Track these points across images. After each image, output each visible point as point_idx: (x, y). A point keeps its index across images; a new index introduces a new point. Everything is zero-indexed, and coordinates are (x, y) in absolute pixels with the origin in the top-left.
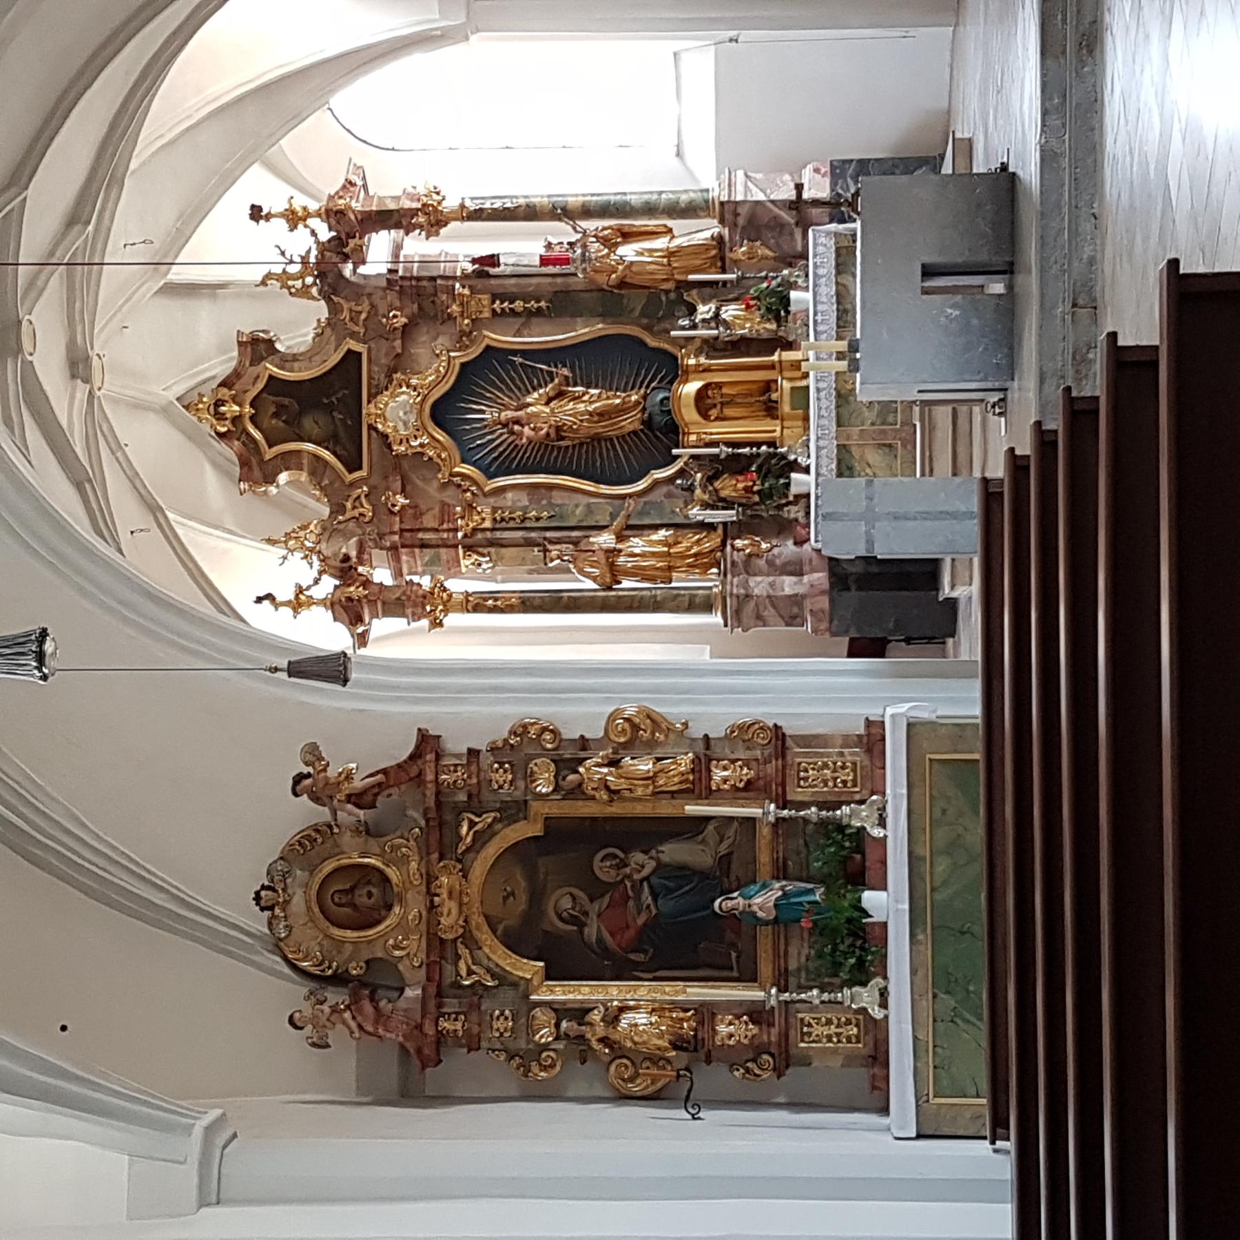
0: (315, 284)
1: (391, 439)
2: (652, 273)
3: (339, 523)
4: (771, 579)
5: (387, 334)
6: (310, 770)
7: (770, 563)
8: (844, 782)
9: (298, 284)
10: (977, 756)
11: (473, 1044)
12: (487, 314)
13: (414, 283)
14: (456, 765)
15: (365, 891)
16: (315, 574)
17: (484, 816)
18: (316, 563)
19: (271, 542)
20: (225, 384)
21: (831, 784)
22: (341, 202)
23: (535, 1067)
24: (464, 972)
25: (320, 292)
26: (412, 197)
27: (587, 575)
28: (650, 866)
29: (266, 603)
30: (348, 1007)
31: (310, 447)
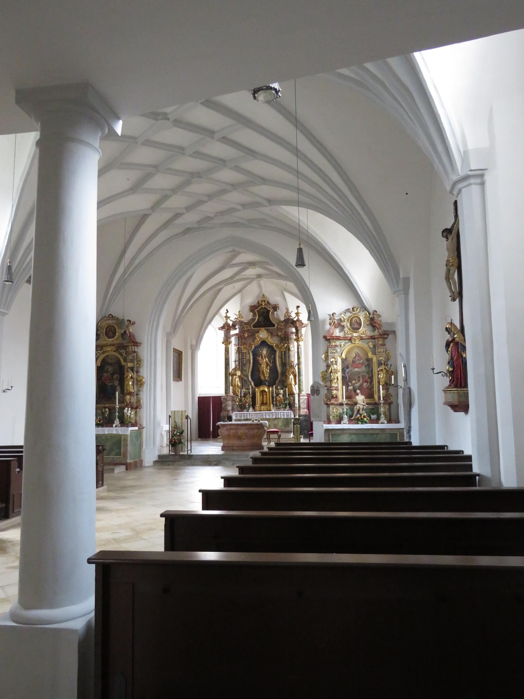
3: (243, 324)
7: (234, 405)
9: (286, 315)
12: (282, 350)
15: (111, 333)
16: (233, 320)
18: (234, 320)
19: (239, 312)
20: (268, 302)
24: (99, 351)
28: (116, 384)
29: (226, 311)
31: (257, 318)
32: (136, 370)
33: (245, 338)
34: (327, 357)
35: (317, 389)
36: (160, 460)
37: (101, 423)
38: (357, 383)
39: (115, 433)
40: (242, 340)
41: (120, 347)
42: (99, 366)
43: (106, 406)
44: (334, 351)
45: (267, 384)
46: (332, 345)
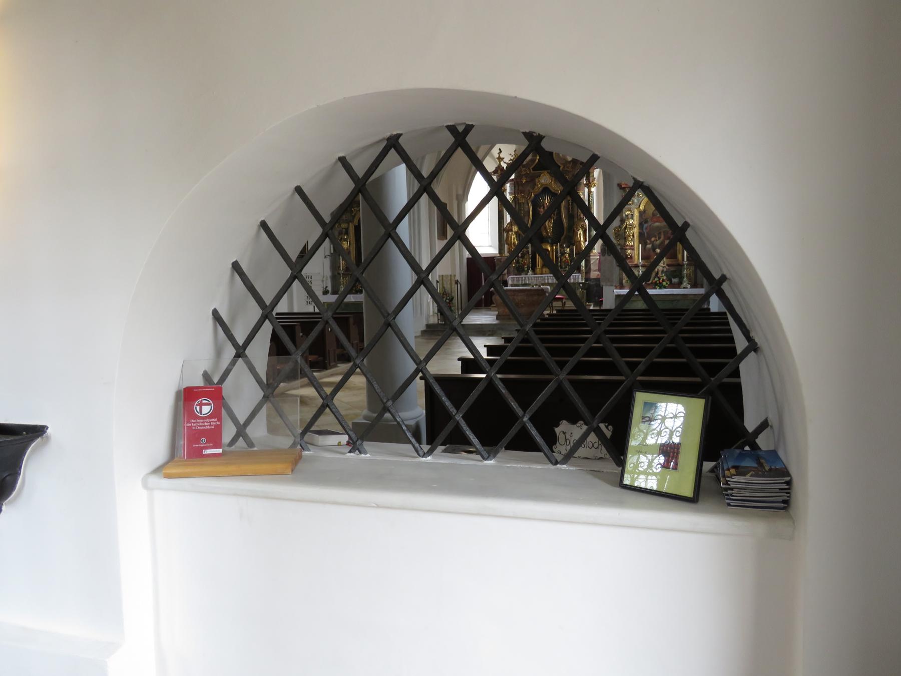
16: (507, 162)
18: (509, 162)
19: (515, 151)
24: (355, 208)
29: (499, 151)
31: (538, 158)
33: (522, 185)
36: (428, 329)
38: (657, 241)
40: (518, 187)
45: (550, 241)
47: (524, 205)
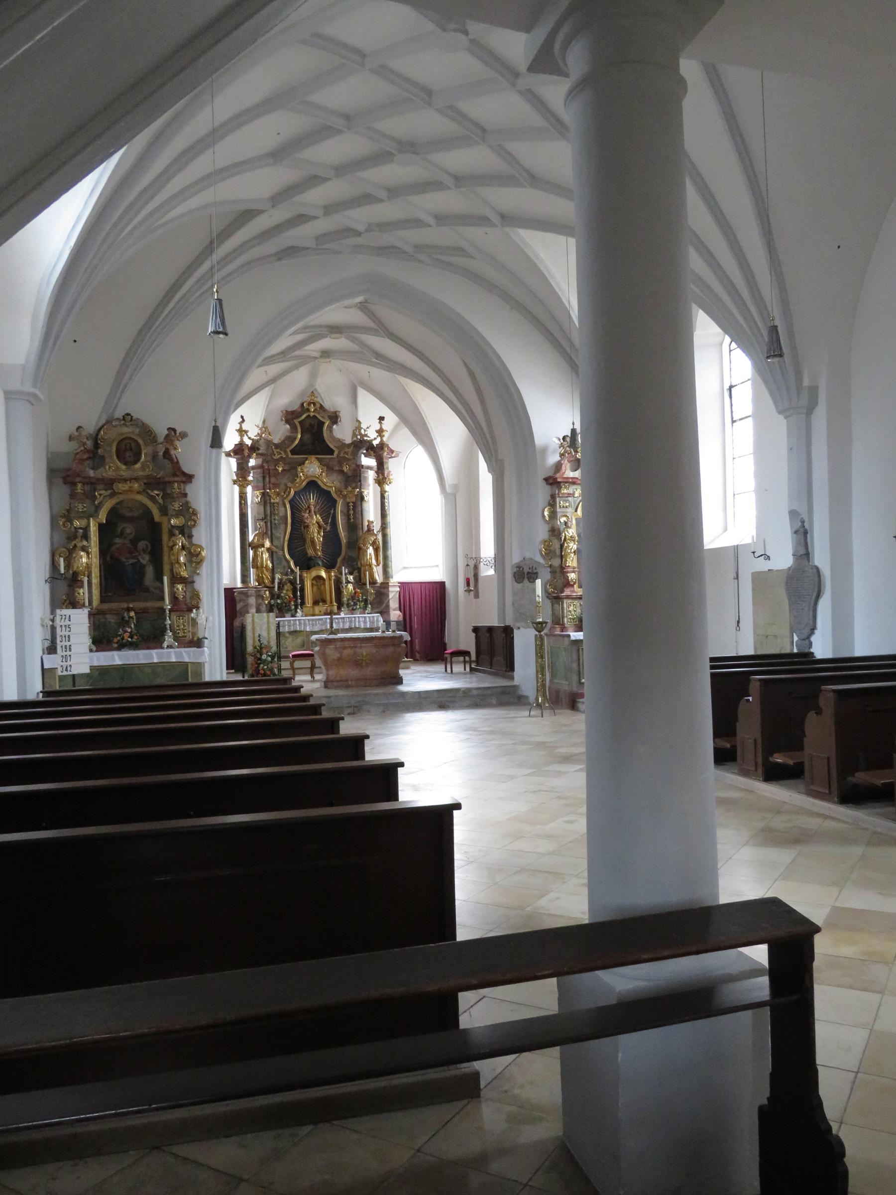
0: (358, 439)
1: (302, 465)
2: (364, 559)
4: (255, 605)
5: (340, 464)
6: (178, 434)
8: (179, 633)
9: (357, 433)
10: (190, 680)
11: (73, 496)
12: (348, 500)
13: (359, 474)
14: (181, 489)
16: (253, 437)
17: (161, 500)
19: (264, 422)
20: (321, 407)
21: (178, 628)
22: (386, 449)
23: (63, 520)
25: (354, 441)
26: (389, 472)
27: (254, 538)
28: (144, 562)
29: (241, 420)
30: (85, 449)
31: (299, 436)
32: (185, 531)
33: (277, 474)
34: (553, 515)
35: (528, 570)
37: (134, 640)
39: (174, 660)
40: (270, 479)
41: (152, 483)
42: (104, 524)
43: (131, 606)
44: (567, 504)
46: (563, 494)
47: (278, 506)
